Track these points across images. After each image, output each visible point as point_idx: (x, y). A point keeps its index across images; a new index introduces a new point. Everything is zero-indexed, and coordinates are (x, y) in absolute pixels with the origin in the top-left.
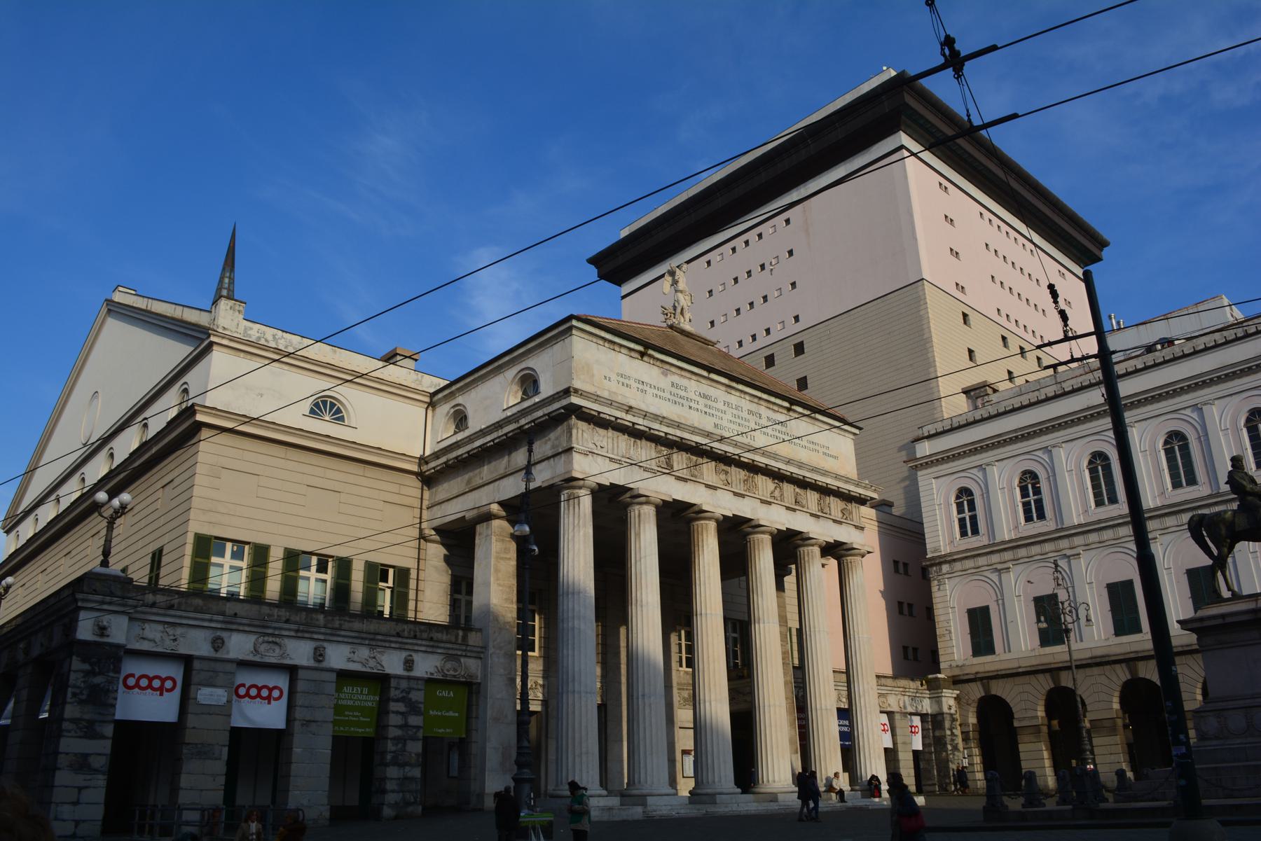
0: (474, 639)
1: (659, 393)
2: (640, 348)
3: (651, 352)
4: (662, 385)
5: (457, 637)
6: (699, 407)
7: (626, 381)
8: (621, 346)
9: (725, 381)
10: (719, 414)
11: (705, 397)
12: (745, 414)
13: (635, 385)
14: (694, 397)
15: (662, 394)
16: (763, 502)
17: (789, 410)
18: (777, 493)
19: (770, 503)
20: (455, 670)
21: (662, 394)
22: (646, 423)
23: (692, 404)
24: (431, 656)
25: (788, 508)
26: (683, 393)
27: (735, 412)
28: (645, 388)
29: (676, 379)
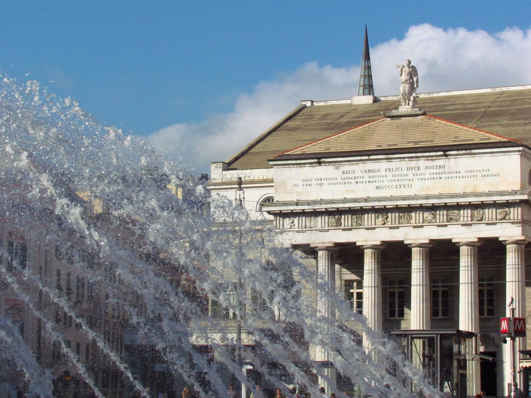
2: (316, 160)
3: (323, 160)
4: (335, 176)
7: (307, 183)
8: (304, 164)
9: (384, 156)
10: (382, 179)
11: (370, 171)
12: (405, 172)
13: (314, 182)
15: (335, 181)
16: (415, 227)
17: (446, 156)
21: (335, 181)
22: (310, 207)
25: (438, 226)
27: (395, 173)
29: (346, 167)
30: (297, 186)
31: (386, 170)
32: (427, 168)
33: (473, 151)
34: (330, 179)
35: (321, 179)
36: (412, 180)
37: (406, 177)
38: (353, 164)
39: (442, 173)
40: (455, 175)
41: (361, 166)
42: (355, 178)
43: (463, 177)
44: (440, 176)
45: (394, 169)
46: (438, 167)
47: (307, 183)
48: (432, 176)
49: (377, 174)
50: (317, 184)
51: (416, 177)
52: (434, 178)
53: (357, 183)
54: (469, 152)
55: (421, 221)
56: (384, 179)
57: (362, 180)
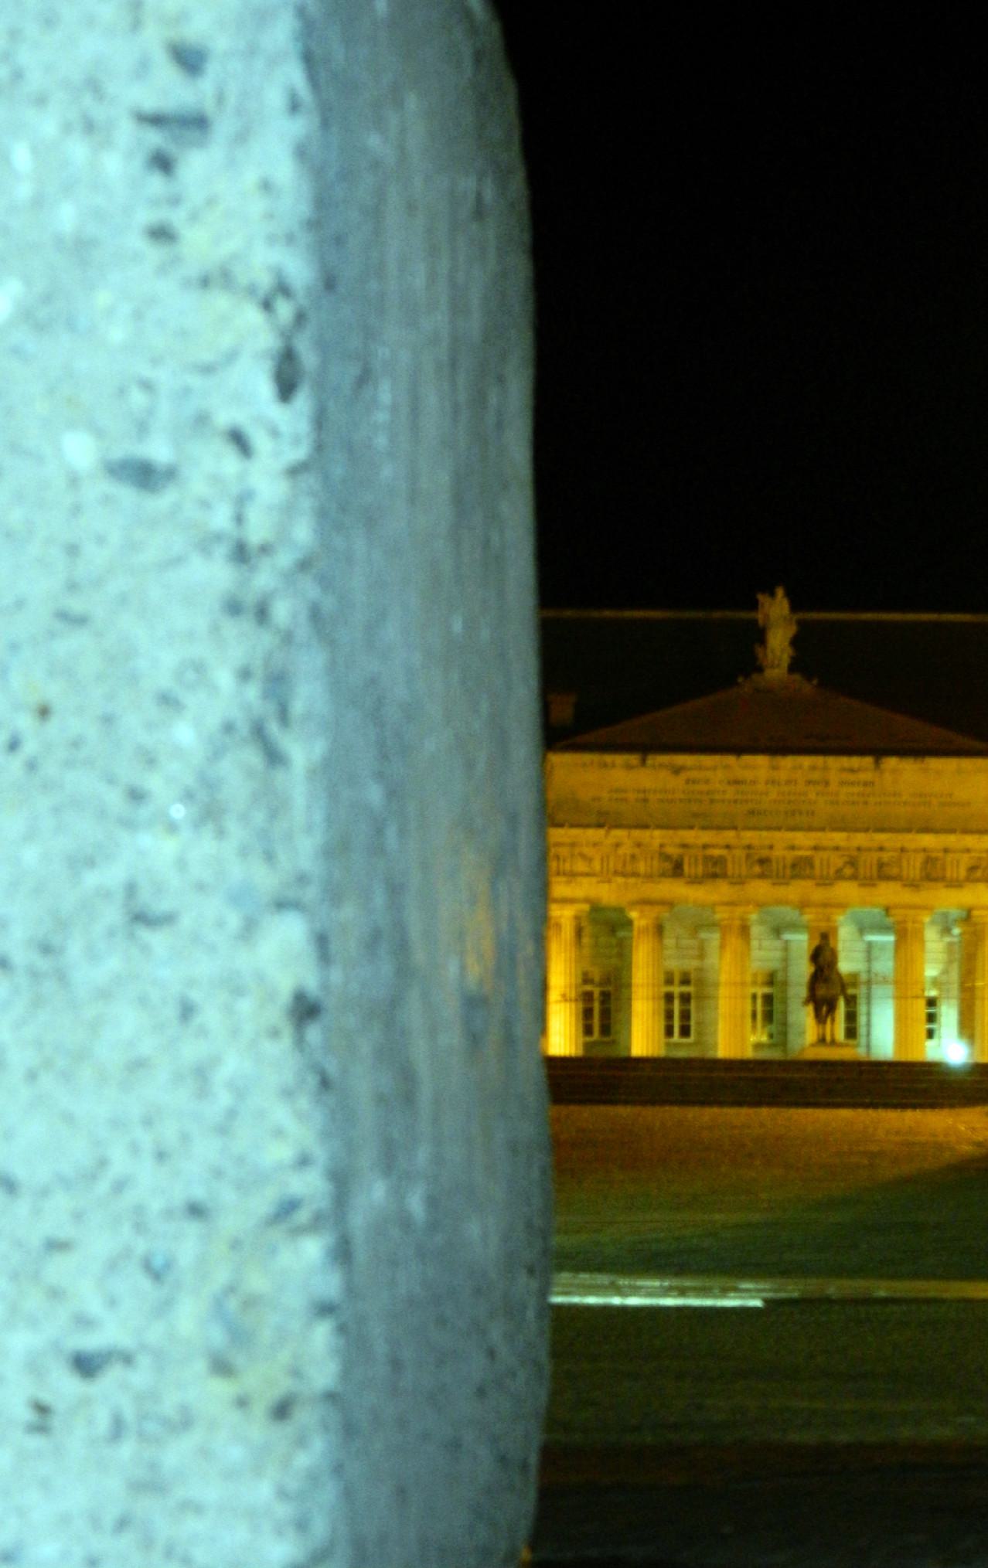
6: (728, 796)
11: (737, 782)
13: (631, 796)
17: (877, 763)
18: (848, 871)
23: (717, 797)
27: (786, 789)
38: (708, 769)
40: (892, 799)
41: (720, 774)
42: (708, 793)
53: (712, 801)
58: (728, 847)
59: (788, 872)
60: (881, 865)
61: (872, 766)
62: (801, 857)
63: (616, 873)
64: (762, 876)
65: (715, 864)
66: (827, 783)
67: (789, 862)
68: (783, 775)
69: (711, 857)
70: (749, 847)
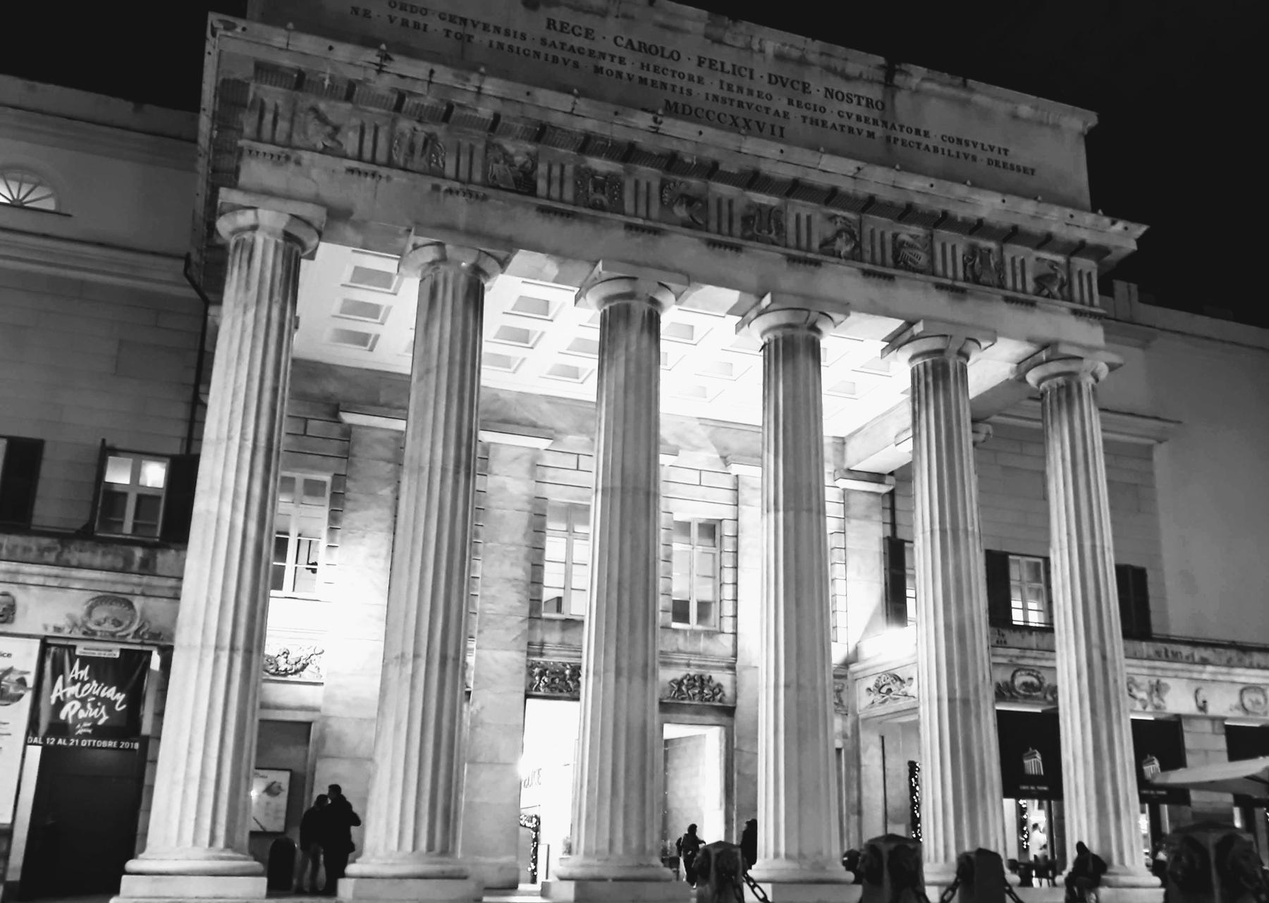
0: (165, 559)
1: (507, 41)
5: (128, 561)
6: (626, 69)
11: (644, 48)
12: (762, 85)
13: (435, 24)
14: (606, 46)
15: (517, 43)
17: (890, 72)
18: (844, 246)
19: (817, 263)
20: (117, 623)
23: (606, 64)
24: (59, 593)
26: (577, 42)
27: (728, 79)
28: (469, 30)
30: (367, 14)
31: (700, 63)
32: (829, 93)
33: (970, 82)
34: (497, 30)
35: (464, 21)
36: (786, 115)
37: (763, 103)
39: (875, 122)
42: (591, 53)
43: (936, 149)
44: (872, 128)
45: (728, 67)
46: (863, 102)
47: (412, 18)
48: (845, 121)
49: (670, 64)
50: (448, 32)
51: (794, 112)
52: (851, 130)
53: (598, 70)
54: (959, 80)
55: (816, 245)
56: (696, 88)
57: (616, 66)
58: (629, 153)
59: (737, 226)
60: (898, 246)
61: (880, 75)
62: (760, 208)
63: (390, 164)
64: (685, 225)
65: (599, 186)
66: (805, 88)
67: (738, 208)
68: (726, 56)
69: (593, 173)
70: (671, 162)
